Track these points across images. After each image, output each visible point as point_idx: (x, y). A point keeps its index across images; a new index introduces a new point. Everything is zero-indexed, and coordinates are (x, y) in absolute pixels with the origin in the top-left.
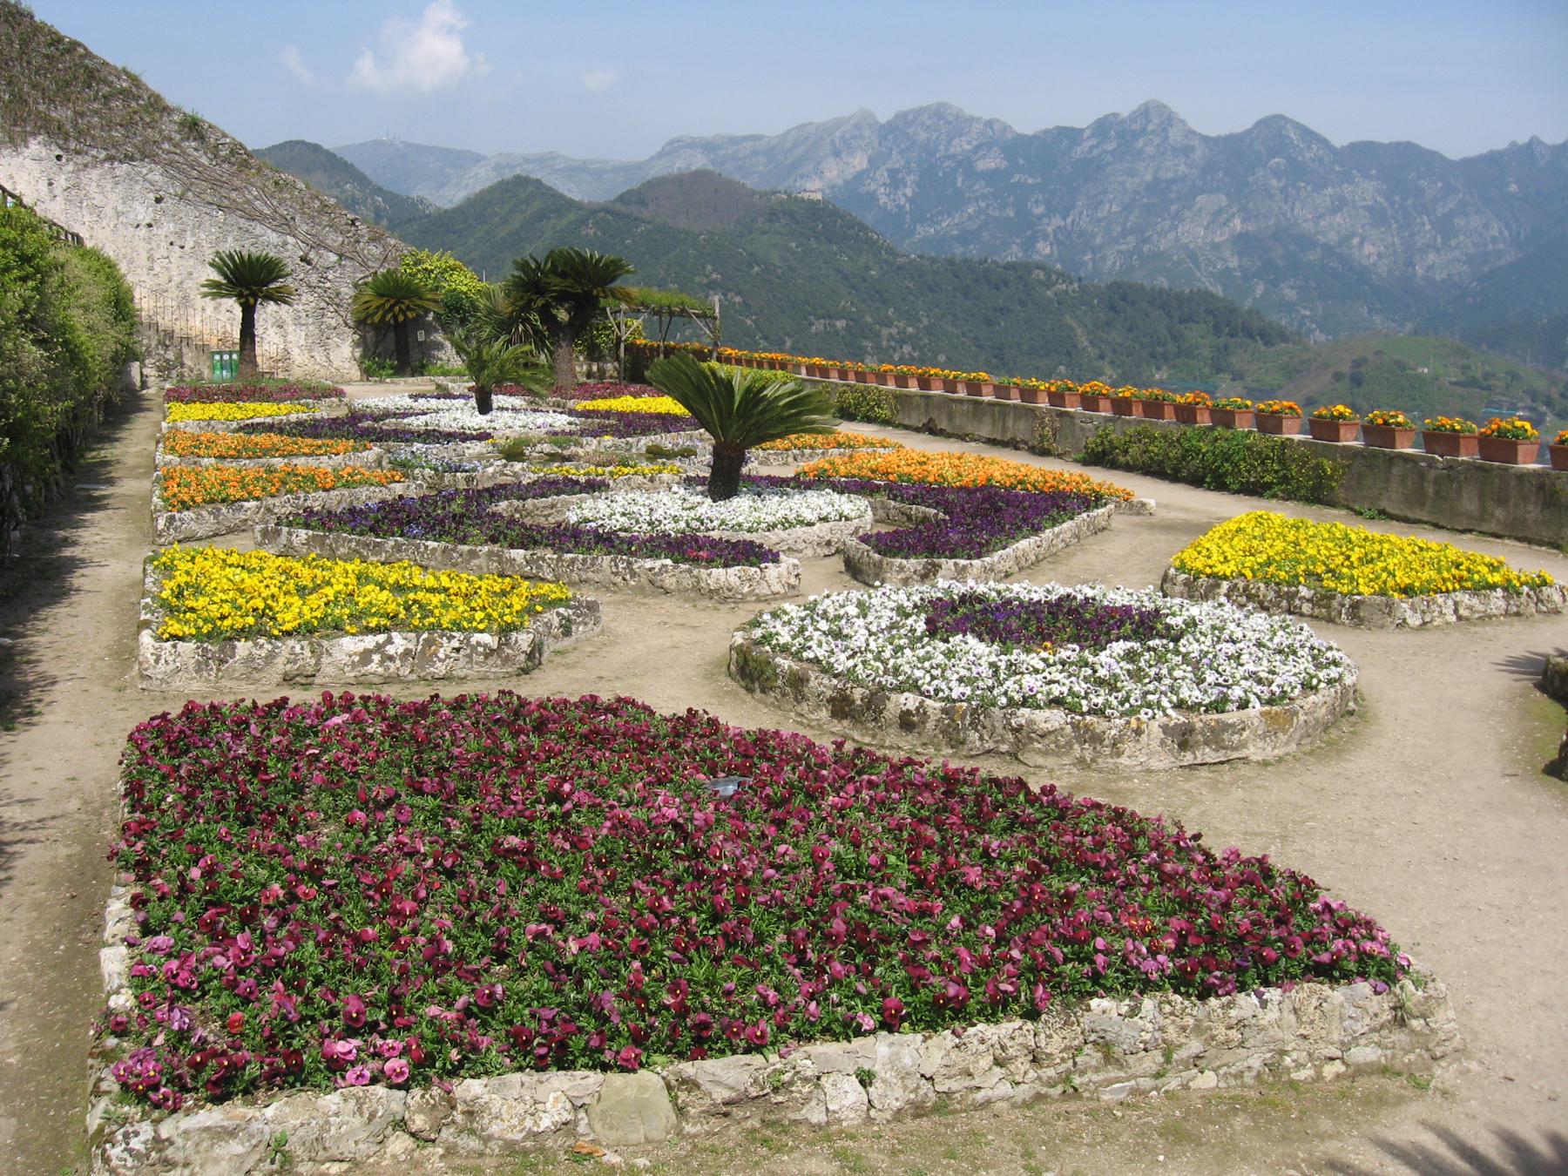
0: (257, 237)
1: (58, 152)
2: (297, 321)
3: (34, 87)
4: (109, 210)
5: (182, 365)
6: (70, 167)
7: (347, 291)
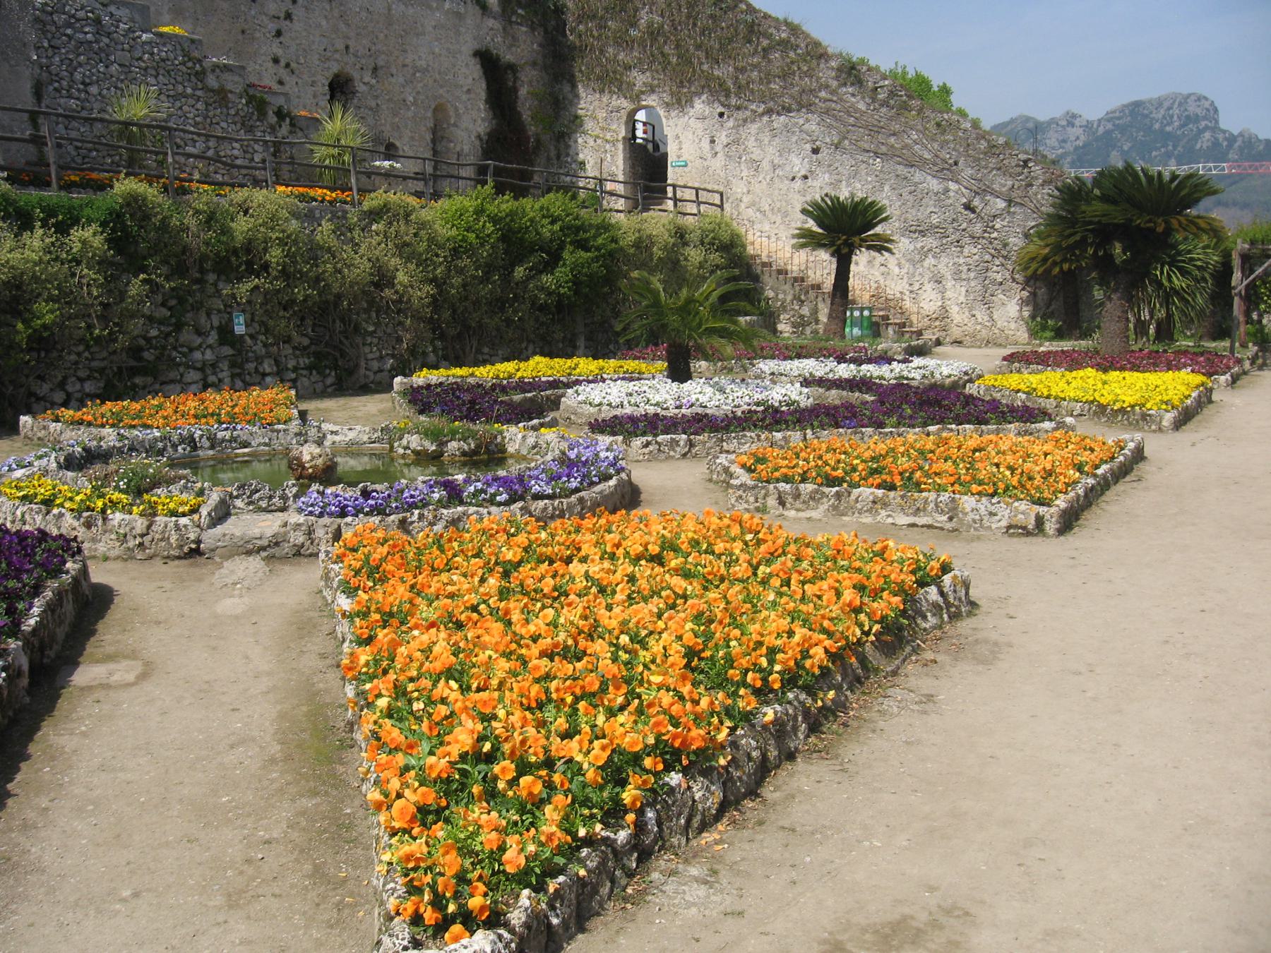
0: (916, 184)
1: (721, 109)
2: (957, 276)
3: (698, 47)
4: (765, 165)
5: (817, 322)
6: (731, 123)
7: (1016, 242)
